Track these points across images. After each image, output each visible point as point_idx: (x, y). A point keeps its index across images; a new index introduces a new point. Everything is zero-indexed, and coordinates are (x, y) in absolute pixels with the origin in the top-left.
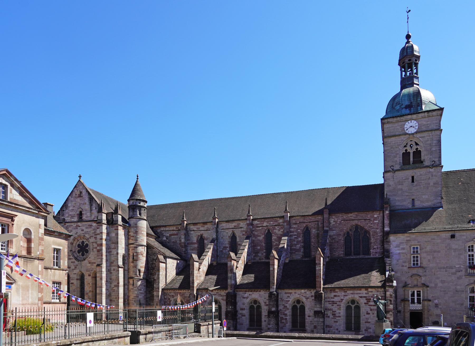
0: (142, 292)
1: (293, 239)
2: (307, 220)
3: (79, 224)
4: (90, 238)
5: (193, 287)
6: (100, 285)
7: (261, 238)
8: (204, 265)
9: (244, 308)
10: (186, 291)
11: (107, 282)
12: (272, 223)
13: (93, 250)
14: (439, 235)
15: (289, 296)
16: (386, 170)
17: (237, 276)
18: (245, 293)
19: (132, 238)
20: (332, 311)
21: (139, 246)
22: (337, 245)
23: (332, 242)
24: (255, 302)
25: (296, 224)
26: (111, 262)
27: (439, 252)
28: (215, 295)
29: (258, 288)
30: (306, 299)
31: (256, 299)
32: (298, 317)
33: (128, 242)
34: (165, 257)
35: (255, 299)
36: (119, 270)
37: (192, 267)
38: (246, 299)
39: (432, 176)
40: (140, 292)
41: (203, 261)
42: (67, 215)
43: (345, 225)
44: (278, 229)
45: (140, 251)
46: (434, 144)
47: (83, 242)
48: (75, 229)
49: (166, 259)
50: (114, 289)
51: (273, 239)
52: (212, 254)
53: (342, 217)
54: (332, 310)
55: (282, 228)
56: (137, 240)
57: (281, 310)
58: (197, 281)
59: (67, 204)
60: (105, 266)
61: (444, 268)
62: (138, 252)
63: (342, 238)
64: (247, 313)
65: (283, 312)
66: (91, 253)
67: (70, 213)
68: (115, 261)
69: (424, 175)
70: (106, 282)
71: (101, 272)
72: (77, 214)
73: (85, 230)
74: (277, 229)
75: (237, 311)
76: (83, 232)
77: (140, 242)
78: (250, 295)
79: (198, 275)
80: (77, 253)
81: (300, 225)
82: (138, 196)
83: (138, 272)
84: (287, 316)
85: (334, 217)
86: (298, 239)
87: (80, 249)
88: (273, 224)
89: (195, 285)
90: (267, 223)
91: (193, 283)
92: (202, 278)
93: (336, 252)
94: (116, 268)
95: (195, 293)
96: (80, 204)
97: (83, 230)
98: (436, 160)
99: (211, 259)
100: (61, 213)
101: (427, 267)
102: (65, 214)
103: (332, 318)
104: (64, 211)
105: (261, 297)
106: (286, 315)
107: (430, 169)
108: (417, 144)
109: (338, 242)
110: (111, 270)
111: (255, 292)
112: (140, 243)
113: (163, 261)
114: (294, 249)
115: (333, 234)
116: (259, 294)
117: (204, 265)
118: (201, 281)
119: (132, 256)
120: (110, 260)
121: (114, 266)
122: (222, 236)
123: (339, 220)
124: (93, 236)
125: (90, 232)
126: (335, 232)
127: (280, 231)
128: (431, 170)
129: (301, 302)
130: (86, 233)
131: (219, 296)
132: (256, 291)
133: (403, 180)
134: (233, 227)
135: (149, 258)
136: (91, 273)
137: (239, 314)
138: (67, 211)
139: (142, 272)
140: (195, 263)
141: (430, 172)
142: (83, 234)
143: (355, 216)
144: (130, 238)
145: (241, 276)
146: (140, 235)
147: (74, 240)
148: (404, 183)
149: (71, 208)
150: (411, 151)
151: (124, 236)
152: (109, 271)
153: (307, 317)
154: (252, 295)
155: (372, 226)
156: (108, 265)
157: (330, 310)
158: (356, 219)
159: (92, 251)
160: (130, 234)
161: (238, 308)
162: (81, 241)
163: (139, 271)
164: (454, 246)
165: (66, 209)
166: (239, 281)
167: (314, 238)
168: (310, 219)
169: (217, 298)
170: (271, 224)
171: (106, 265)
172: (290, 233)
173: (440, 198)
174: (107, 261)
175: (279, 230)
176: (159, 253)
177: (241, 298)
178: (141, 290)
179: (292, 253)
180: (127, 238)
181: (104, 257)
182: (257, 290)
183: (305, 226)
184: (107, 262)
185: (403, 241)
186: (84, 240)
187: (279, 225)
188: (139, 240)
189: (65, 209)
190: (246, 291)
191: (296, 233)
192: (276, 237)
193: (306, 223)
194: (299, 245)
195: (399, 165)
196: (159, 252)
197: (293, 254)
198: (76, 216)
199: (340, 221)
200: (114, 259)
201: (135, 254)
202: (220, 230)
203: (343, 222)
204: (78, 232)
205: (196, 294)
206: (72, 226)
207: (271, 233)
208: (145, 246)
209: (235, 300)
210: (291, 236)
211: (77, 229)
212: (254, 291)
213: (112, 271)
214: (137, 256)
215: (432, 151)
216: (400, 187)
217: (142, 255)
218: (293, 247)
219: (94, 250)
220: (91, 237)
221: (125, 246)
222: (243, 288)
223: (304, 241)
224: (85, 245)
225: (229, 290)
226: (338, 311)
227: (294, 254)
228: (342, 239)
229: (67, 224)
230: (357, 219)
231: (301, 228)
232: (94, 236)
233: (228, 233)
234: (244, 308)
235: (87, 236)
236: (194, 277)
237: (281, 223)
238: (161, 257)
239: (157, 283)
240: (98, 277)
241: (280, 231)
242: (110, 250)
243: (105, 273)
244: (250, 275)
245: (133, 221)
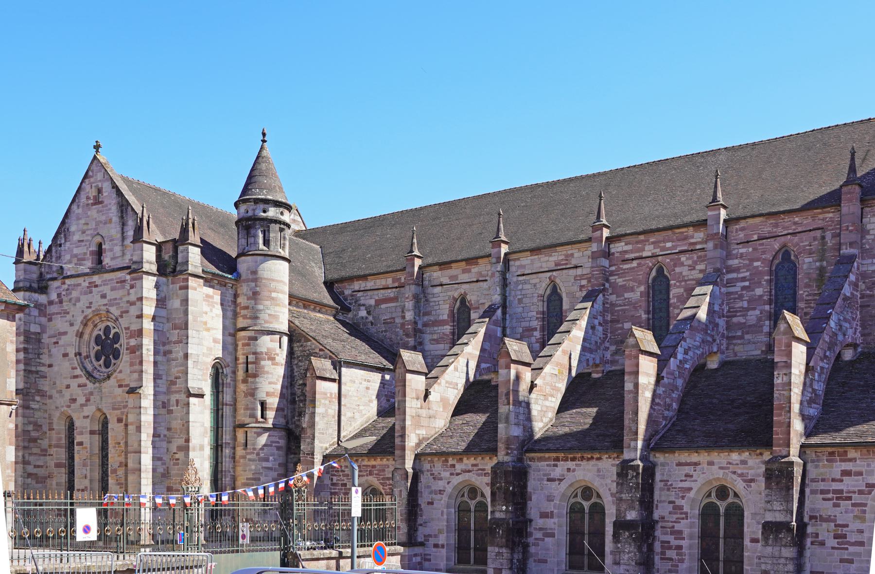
0: (269, 465)
1: (736, 293)
3: (96, 278)
4: (121, 316)
5: (403, 448)
6: (136, 445)
7: (637, 294)
8: (447, 382)
9: (552, 512)
10: (388, 460)
11: (157, 439)
12: (669, 245)
15: (692, 473)
17: (534, 413)
18: (556, 466)
19: (243, 312)
20: (836, 526)
21: (264, 334)
24: (587, 492)
25: (748, 242)
26: (172, 378)
28: (469, 471)
29: (593, 449)
30: (744, 484)
31: (590, 485)
32: (721, 541)
33: (235, 324)
34: (337, 365)
35: (583, 484)
36: (188, 404)
37: (400, 388)
38: (557, 482)
40: (265, 464)
41: (444, 371)
42: (68, 257)
44: (690, 262)
45: (264, 350)
47: (107, 330)
48: (86, 294)
49: (340, 369)
50: (177, 456)
51: (671, 296)
52: (483, 350)
54: (835, 521)
55: (701, 259)
56: (257, 318)
57: (663, 518)
58: (418, 432)
59: (67, 225)
60: (152, 392)
62: (259, 350)
64: (560, 526)
65: (671, 524)
67: (76, 251)
68: (179, 378)
70: (154, 436)
71: (138, 410)
72: (92, 253)
73: (111, 295)
74: (685, 264)
75: (531, 521)
76: (105, 301)
77: (266, 322)
78: (569, 470)
79: (424, 413)
80: (93, 360)
82: (261, 189)
83: (259, 407)
84: (683, 539)
86: (753, 290)
87: (99, 348)
89: (411, 441)
90: (654, 248)
91: (403, 436)
92: (441, 422)
94: (182, 397)
95: (409, 465)
96: (98, 223)
97: (104, 296)
99: (478, 366)
100: (54, 254)
102: (63, 253)
103: (833, 548)
104: (60, 245)
105: (603, 477)
106: (678, 534)
110: (171, 403)
111: (584, 463)
112: (266, 325)
113: (328, 376)
114: (740, 324)
116: (596, 468)
117: (447, 382)
118: (433, 432)
119: (243, 363)
120: (168, 375)
121: (176, 392)
122: (520, 297)
125: (121, 299)
127: (694, 269)
129: (731, 494)
130: (113, 302)
131: (481, 475)
132: (588, 459)
134: (552, 266)
135: (296, 370)
136: (122, 413)
137: (535, 529)
138: (68, 244)
139: (271, 409)
140: (409, 376)
144: (240, 313)
145: (551, 414)
146: (268, 303)
147: (86, 325)
149: (76, 237)
151: (219, 307)
152: (162, 406)
153: (747, 542)
154: (574, 470)
156: (163, 389)
157: (828, 520)
160: (239, 300)
161: (533, 511)
162: (102, 326)
163: (263, 404)
165: (65, 241)
166: (541, 429)
167: (807, 286)
169: (473, 480)
170: (669, 249)
171: (155, 391)
172: (728, 272)
174: (157, 377)
175: (692, 268)
176: (321, 353)
177: (543, 480)
178: (267, 460)
179: (734, 337)
180: (230, 314)
181: (148, 368)
182: (589, 456)
184: (158, 381)
186: (109, 324)
187: (692, 250)
188: (263, 316)
189: (63, 241)
190: (557, 459)
191: (748, 274)
192: (682, 290)
194: (757, 312)
196: (321, 350)
197: (734, 342)
198: (88, 259)
200: (178, 372)
201: (251, 358)
202: (515, 279)
204: (94, 301)
205: (413, 468)
206: (79, 285)
207: (666, 277)
208: (281, 334)
209: (525, 486)
210: (731, 283)
211: (91, 292)
212: (582, 458)
213: (173, 406)
214: (256, 362)
217: (272, 359)
218: (735, 320)
220: (124, 315)
221: (223, 335)
222: (549, 450)
223: (776, 295)
224: (111, 336)
225: (502, 456)
226: (855, 525)
227: (739, 341)
229: (68, 281)
231: (763, 257)
233: (538, 286)
234: (552, 512)
235: (115, 311)
236: (404, 420)
237: (700, 243)
238: (323, 365)
239: (307, 440)
240: (132, 424)
241: (694, 269)
242: (167, 348)
243: (151, 411)
244: (584, 410)
245: (245, 264)
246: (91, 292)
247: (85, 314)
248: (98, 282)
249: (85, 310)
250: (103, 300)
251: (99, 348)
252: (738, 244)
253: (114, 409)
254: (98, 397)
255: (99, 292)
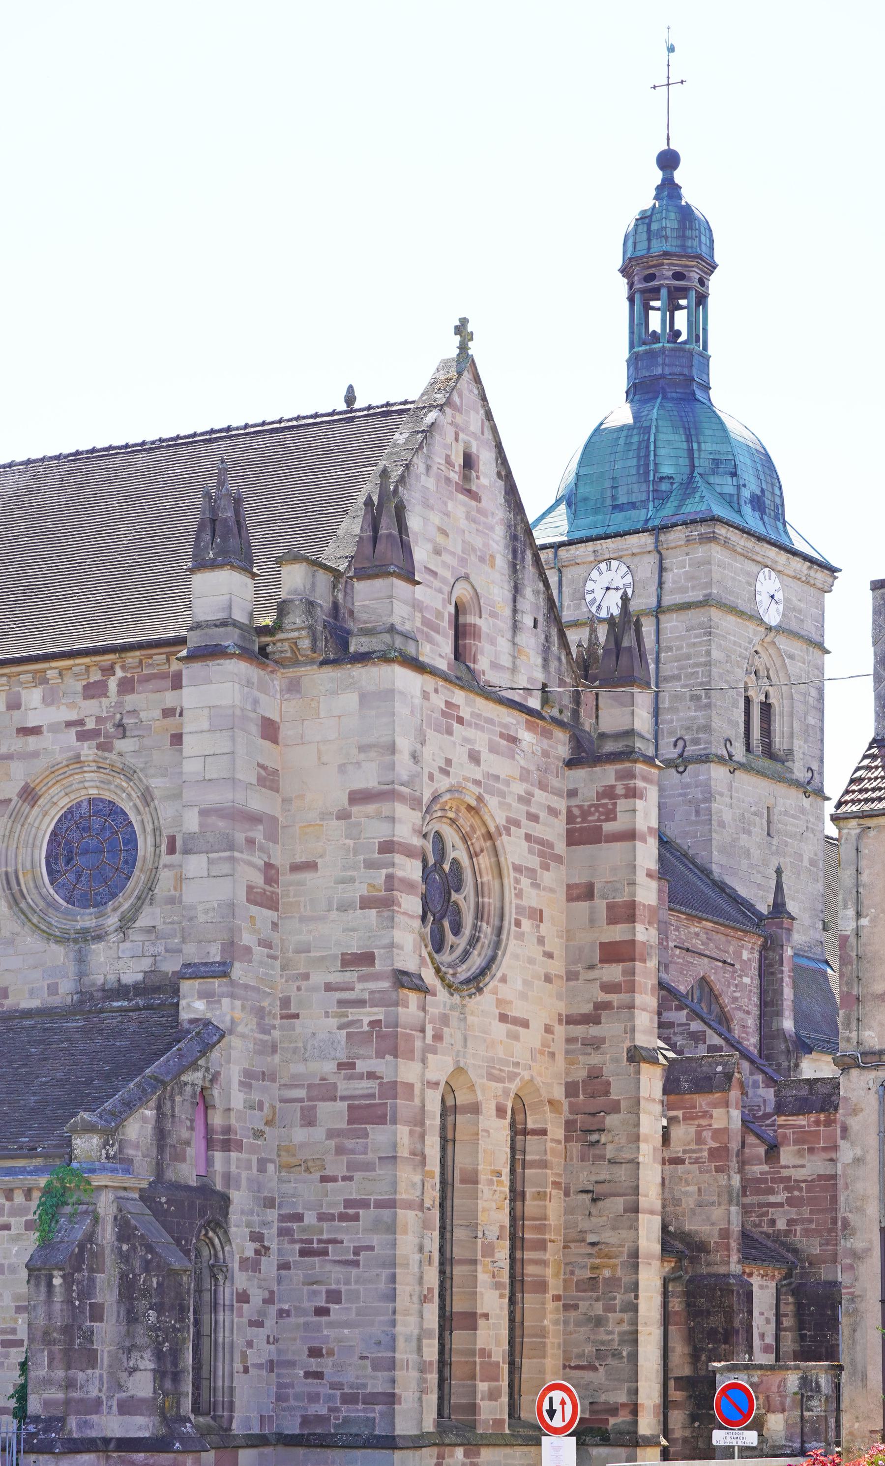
13: (518, 924)
66: (512, 942)
124: (517, 824)
142: (477, 790)
159: (513, 928)
219: (526, 924)
220: (513, 828)
232: (524, 821)
246: (450, 732)
247: (436, 785)
248: (465, 713)
249: (437, 775)
250: (473, 766)
251: (454, 896)
253: (492, 1077)
254: (459, 1036)
255: (466, 740)
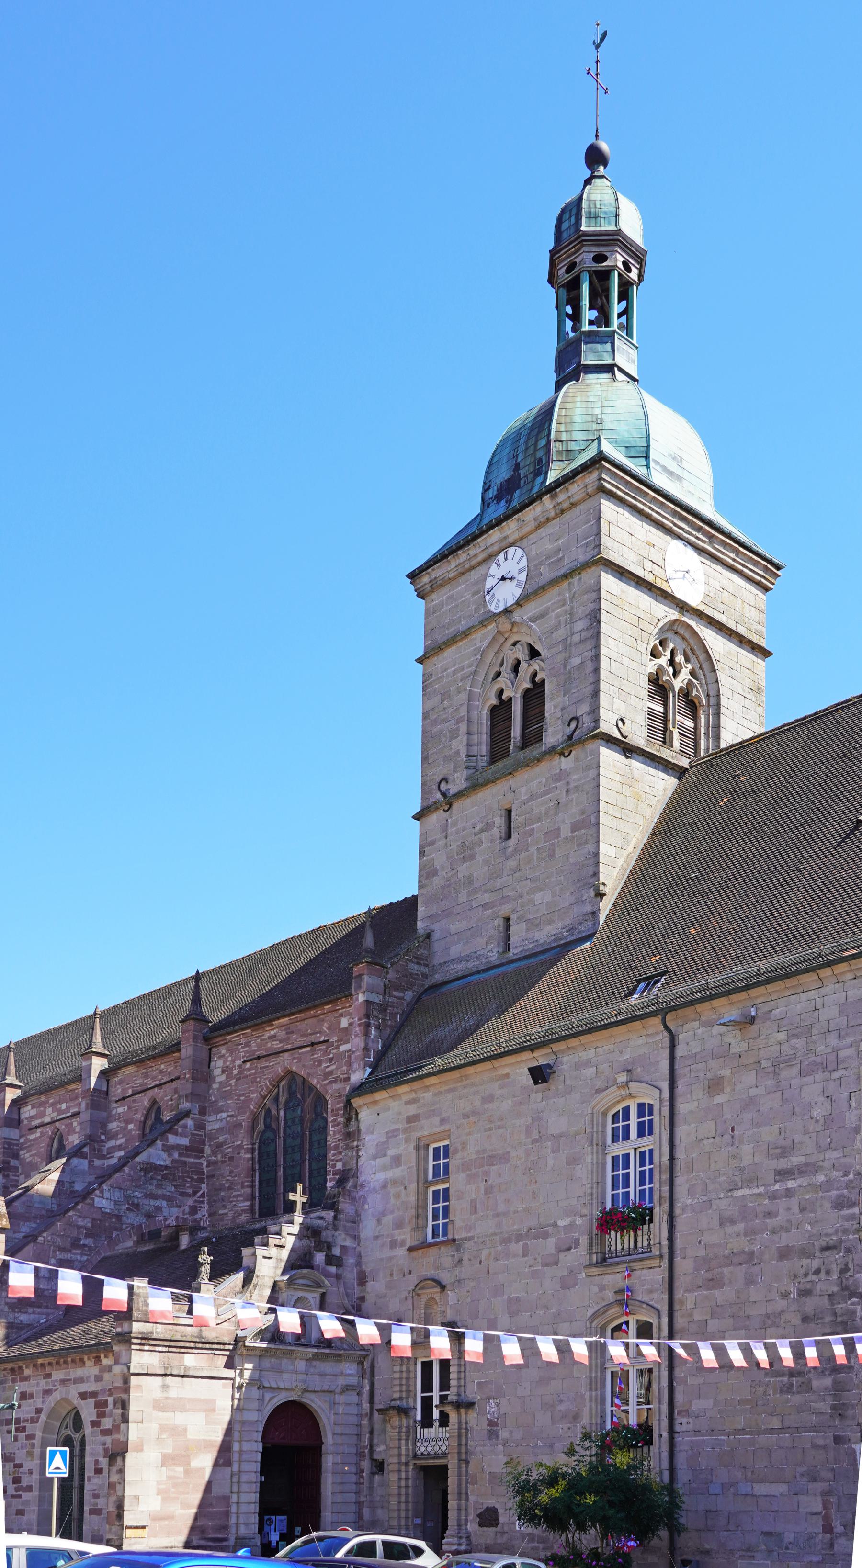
2: (154, 1078)
14: (507, 1075)
16: (425, 804)
22: (231, 1172)
23: (216, 1163)
25: (124, 1099)
27: (505, 1158)
39: (567, 791)
43: (254, 1082)
46: (576, 638)
53: (247, 1045)
61: (519, 1238)
63: (243, 1140)
69: (545, 793)
81: (135, 1101)
85: (223, 1052)
88: (68, 1108)
93: (225, 1207)
98: (583, 710)
101: (466, 1239)
107: (563, 758)
108: (534, 653)
109: (231, 1159)
115: (216, 1127)
123: (238, 1063)
126: (224, 1115)
128: (566, 763)
133: (476, 835)
141: (561, 776)
143: (282, 1034)
148: (477, 850)
150: (515, 693)
155: (331, 1073)
158: (286, 1047)
164: (556, 1124)
168: (161, 1072)
173: (592, 893)
183: (146, 1103)
185: (396, 1127)
193: (150, 1093)
195: (467, 768)
199: (240, 1066)
203: (249, 1069)
215: (570, 672)
216: (463, 870)
228: (247, 1144)
230: (289, 1047)
252: (117, 1101)
